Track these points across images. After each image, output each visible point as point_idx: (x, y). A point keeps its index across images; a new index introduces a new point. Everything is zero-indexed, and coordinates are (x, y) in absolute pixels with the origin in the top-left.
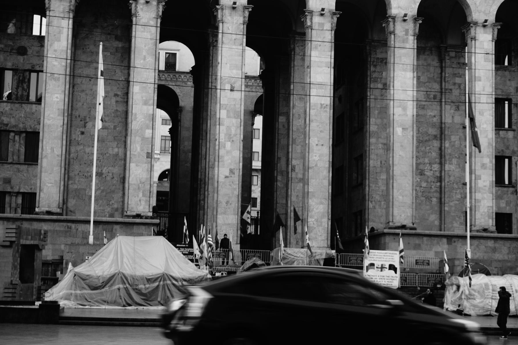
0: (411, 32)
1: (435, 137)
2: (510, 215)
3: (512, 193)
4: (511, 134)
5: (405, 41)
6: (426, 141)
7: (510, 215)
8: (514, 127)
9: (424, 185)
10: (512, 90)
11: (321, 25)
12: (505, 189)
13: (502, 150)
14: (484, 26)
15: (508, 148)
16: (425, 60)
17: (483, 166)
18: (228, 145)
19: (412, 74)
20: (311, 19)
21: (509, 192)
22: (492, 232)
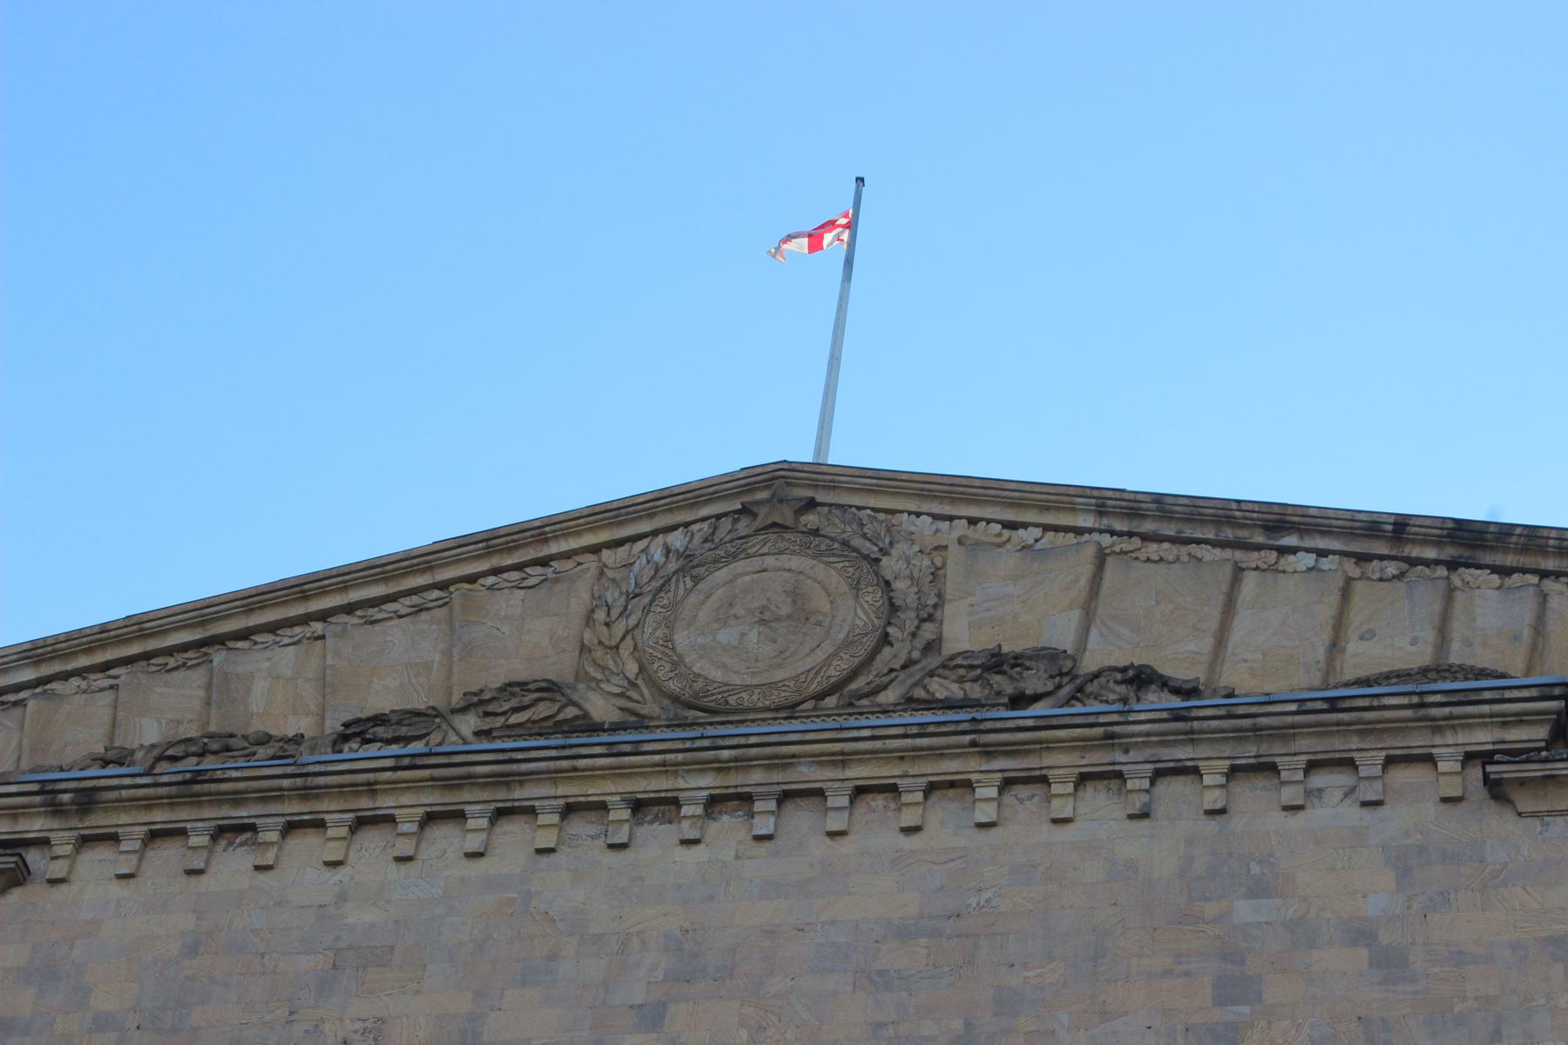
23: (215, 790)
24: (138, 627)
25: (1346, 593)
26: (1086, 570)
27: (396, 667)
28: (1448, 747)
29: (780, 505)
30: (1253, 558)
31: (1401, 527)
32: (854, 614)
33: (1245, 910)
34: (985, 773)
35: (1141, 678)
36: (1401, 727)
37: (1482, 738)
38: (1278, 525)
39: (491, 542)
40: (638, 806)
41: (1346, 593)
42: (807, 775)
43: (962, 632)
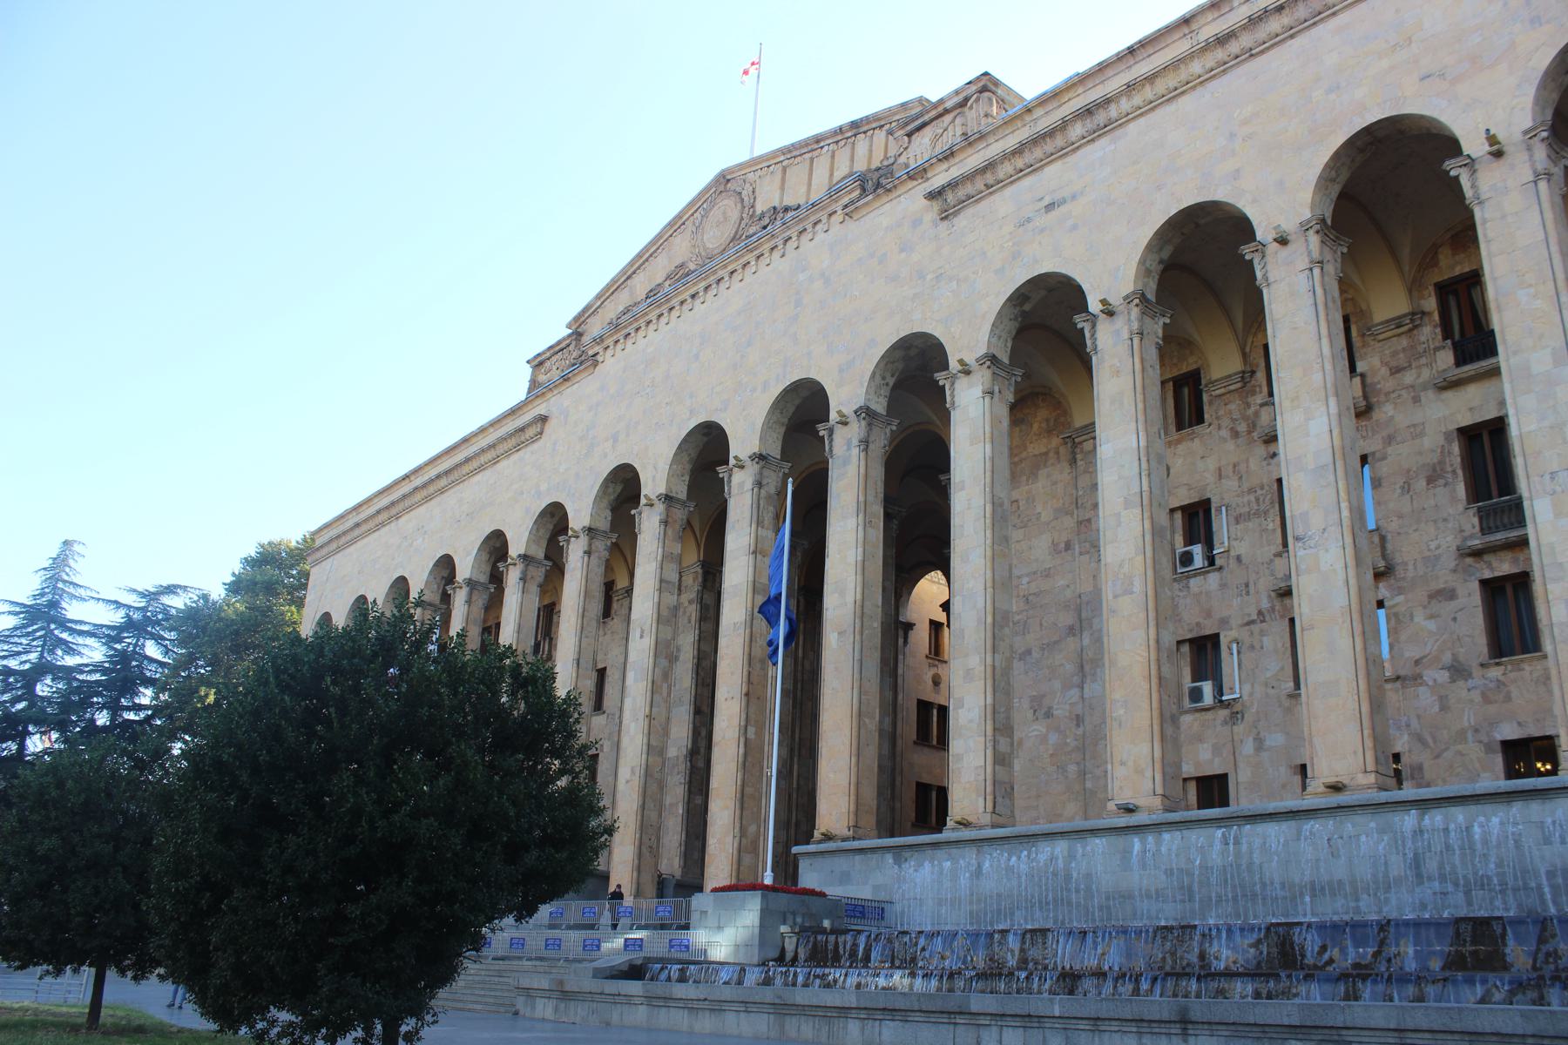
0: (855, 442)
1: (1071, 630)
2: (1223, 778)
3: (1225, 722)
4: (1213, 579)
5: (846, 462)
6: (1056, 643)
7: (1223, 778)
8: (1218, 562)
9: (1053, 738)
10: (1210, 478)
11: (741, 485)
12: (1209, 715)
13: (1198, 624)
14: (968, 373)
15: (1209, 615)
16: (1048, 476)
17: (968, 674)
18: (633, 725)
19: (854, 520)
20: (730, 481)
21: (1219, 722)
22: (981, 827)
23: (624, 327)
24: (614, 281)
25: (833, 157)
26: (778, 176)
27: (659, 270)
28: (838, 207)
29: (723, 181)
30: (815, 153)
31: (841, 129)
32: (734, 215)
33: (801, 277)
34: (750, 257)
35: (786, 209)
36: (829, 205)
37: (846, 200)
38: (818, 139)
39: (671, 224)
40: (693, 296)
41: (833, 157)
42: (720, 273)
43: (760, 208)
